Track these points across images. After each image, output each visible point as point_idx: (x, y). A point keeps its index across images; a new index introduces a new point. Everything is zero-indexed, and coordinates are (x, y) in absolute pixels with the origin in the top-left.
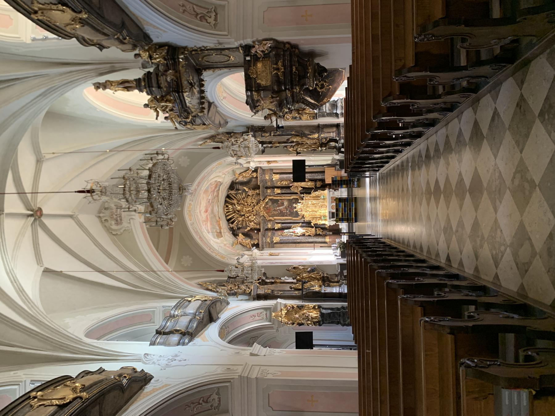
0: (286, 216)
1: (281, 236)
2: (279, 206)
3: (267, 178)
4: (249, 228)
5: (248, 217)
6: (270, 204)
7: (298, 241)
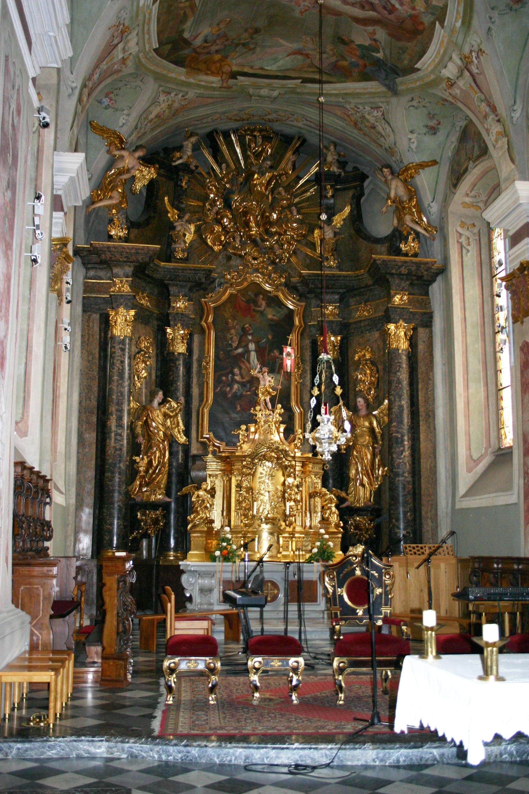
0: (217, 381)
1: (134, 349)
2: (260, 352)
3: (397, 299)
4: (172, 214)
5: (219, 222)
6: (271, 314)
7: (113, 423)
